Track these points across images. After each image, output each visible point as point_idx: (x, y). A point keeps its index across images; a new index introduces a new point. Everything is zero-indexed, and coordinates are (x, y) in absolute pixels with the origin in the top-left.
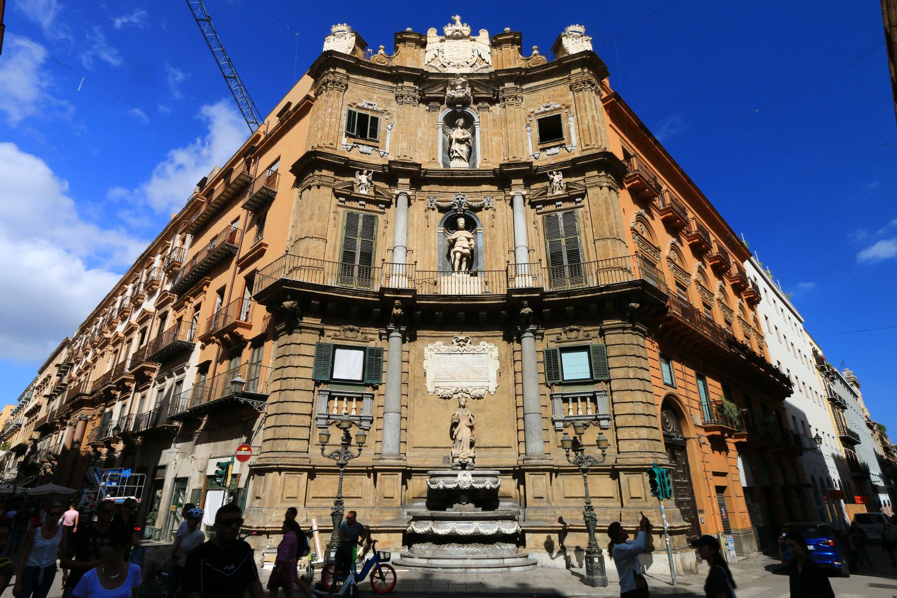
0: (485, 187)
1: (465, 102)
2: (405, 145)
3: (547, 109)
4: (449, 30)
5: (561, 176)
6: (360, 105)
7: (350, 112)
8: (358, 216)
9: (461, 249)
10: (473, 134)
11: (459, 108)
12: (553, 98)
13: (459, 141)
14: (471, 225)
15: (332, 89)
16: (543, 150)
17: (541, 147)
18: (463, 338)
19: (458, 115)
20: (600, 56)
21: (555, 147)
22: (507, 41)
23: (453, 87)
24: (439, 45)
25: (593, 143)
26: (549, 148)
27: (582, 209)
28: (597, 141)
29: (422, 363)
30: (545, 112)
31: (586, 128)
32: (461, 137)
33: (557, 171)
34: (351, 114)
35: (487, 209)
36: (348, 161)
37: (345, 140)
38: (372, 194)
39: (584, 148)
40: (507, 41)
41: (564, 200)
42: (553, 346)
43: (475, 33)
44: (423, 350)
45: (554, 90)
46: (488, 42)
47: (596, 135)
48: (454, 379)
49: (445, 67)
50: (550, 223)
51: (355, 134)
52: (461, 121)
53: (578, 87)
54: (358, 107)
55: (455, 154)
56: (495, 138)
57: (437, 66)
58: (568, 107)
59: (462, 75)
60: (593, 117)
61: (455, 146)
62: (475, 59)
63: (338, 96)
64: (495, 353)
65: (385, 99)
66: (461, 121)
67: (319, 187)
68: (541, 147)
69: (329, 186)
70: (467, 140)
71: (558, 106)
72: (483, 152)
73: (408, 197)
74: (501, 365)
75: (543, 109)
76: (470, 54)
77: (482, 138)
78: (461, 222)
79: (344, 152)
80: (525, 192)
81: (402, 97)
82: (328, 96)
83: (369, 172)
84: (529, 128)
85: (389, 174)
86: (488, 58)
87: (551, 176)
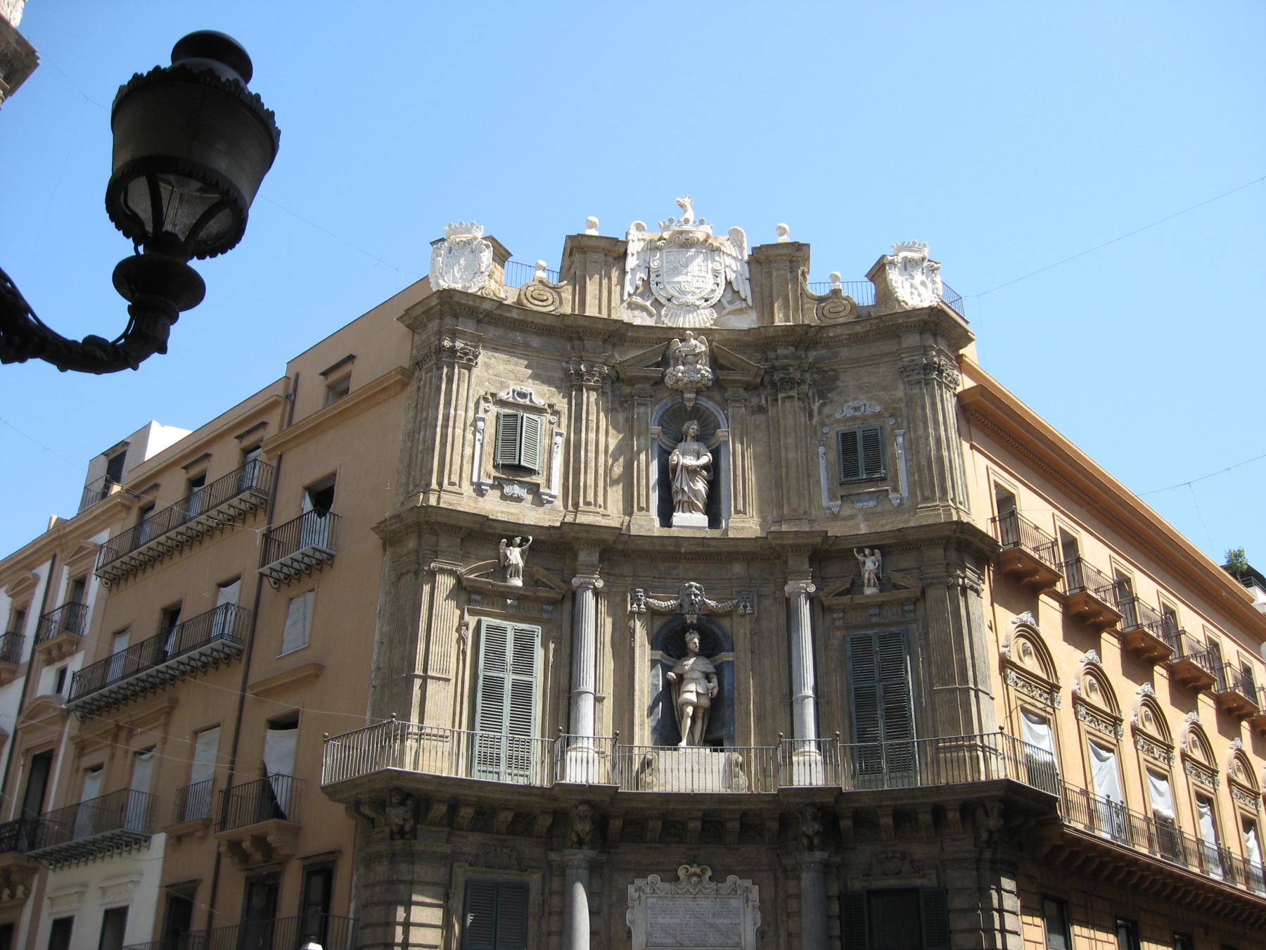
0: (738, 568)
6: (503, 395)
8: (504, 630)
10: (716, 453)
11: (690, 400)
13: (692, 472)
14: (710, 649)
18: (698, 870)
27: (914, 626)
31: (924, 463)
33: (872, 548)
35: (743, 616)
42: (857, 885)
52: (693, 427)
53: (915, 377)
54: (502, 403)
57: (648, 304)
58: (892, 415)
59: (699, 332)
61: (681, 483)
64: (755, 894)
66: (693, 427)
69: (451, 573)
70: (705, 467)
71: (878, 409)
73: (597, 593)
74: (763, 918)
75: (849, 413)
78: (694, 641)
80: (812, 589)
83: (525, 540)
84: (821, 450)
87: (860, 557)
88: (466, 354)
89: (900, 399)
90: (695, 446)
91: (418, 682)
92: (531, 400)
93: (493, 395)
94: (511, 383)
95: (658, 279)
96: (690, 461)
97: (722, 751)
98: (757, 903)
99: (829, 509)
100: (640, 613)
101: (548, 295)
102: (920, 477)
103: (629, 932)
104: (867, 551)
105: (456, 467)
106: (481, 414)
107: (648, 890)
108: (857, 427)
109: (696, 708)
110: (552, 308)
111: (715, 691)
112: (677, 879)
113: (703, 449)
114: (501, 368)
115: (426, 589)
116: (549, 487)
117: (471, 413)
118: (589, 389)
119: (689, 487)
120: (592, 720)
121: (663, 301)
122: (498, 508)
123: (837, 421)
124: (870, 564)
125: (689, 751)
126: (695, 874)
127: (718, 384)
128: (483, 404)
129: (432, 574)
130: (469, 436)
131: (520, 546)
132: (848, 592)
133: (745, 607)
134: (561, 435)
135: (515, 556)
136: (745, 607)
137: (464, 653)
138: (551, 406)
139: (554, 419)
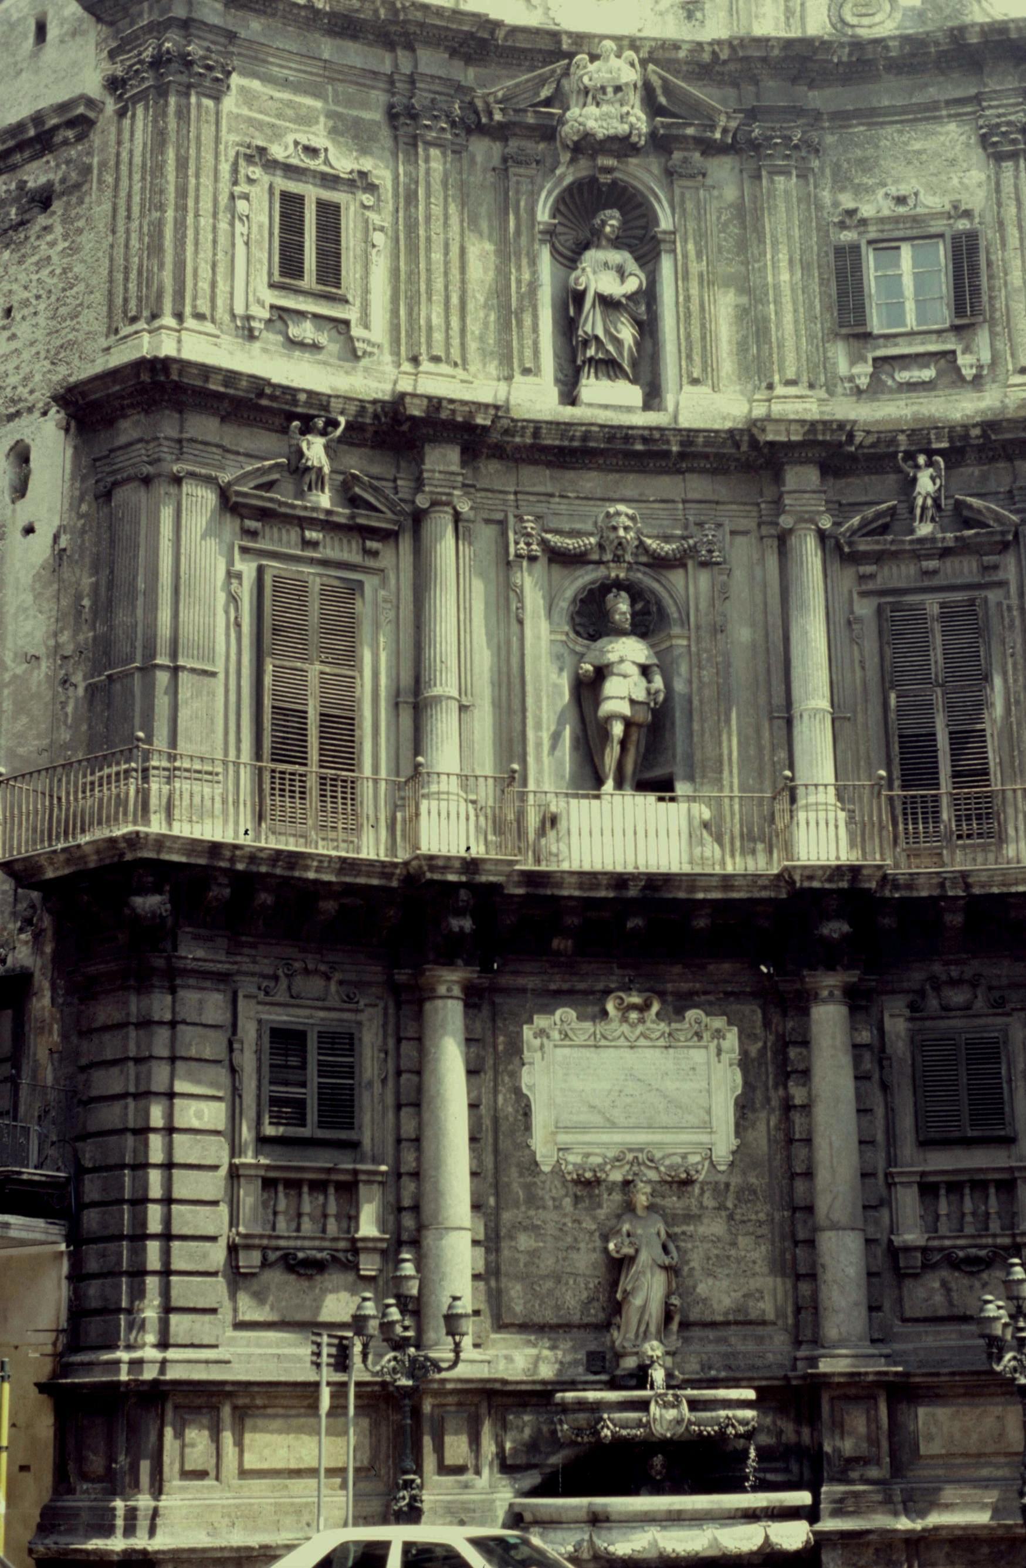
0: (698, 486)
6: (277, 152)
9: (626, 709)
14: (647, 623)
29: (515, 1075)
44: (520, 1034)
48: (612, 1125)
50: (897, 624)
52: (612, 221)
61: (593, 323)
66: (612, 221)
69: (209, 480)
78: (622, 607)
85: (396, 431)
88: (209, 68)
90: (617, 257)
91: (162, 678)
92: (327, 162)
96: (609, 285)
97: (672, 799)
98: (736, 1056)
100: (532, 559)
103: (528, 1106)
105: (204, 286)
106: (243, 188)
107: (556, 1035)
109: (628, 723)
111: (661, 697)
112: (605, 1013)
113: (632, 266)
115: (166, 515)
116: (367, 327)
117: (224, 187)
118: (428, 144)
119: (607, 331)
120: (455, 748)
125: (617, 799)
126: (634, 1007)
127: (660, 143)
128: (245, 169)
129: (177, 480)
130: (223, 226)
131: (323, 433)
132: (884, 529)
133: (710, 551)
134: (382, 229)
136: (710, 551)
137: (238, 625)
138: (363, 174)
139: (367, 199)
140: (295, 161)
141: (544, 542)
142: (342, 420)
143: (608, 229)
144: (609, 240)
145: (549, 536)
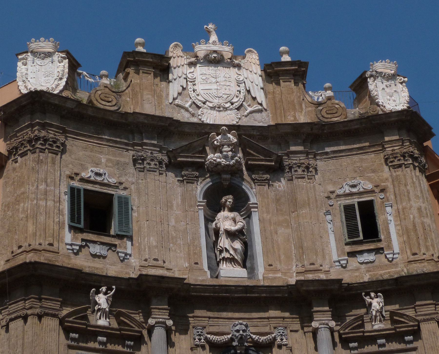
1: (234, 171)
2: (153, 241)
3: (354, 190)
4: (201, 49)
5: (380, 300)
6: (84, 175)
7: (72, 190)
11: (225, 180)
12: (361, 173)
15: (42, 151)
16: (352, 254)
17: (348, 249)
19: (225, 190)
20: (426, 115)
21: (369, 251)
22: (286, 73)
23: (217, 149)
24: (188, 70)
25: (423, 250)
26: (361, 252)
28: (427, 249)
30: (351, 194)
31: (411, 227)
32: (234, 228)
33: (376, 292)
34: (74, 193)
35: (280, 347)
36: (78, 273)
37: (68, 237)
38: (115, 325)
39: (412, 258)
40: (286, 73)
41: (389, 338)
43: (239, 52)
45: (362, 160)
46: (258, 69)
47: (426, 239)
49: (199, 107)
51: (82, 226)
52: (229, 200)
53: (396, 163)
54: (82, 180)
55: (225, 255)
56: (281, 230)
57: (187, 105)
58: (382, 191)
59: (231, 128)
60: (419, 209)
62: (242, 96)
63: (54, 163)
65: (118, 163)
66: (229, 200)
67: (40, 317)
68: (348, 249)
71: (369, 186)
72: (266, 253)
73: (168, 331)
75: (347, 190)
76: (234, 89)
77: (263, 231)
79: (69, 257)
81: (143, 160)
82: (39, 162)
84: (329, 217)
86: (261, 97)
87: (368, 299)
89: (387, 179)
93: (77, 174)
94: (89, 165)
95: (195, 87)
99: (339, 261)
101: (111, 97)
102: (408, 237)
104: (373, 294)
108: (355, 201)
110: (115, 108)
113: (238, 218)
114: (81, 153)
121: (199, 103)
122: (86, 264)
123: (339, 196)
124: (377, 303)
131: (105, 294)
133: (282, 340)
135: (102, 300)
136: (282, 340)
140: (92, 179)
141: (206, 339)
142: (114, 287)
143: (228, 203)
144: (228, 207)
145: (209, 336)
